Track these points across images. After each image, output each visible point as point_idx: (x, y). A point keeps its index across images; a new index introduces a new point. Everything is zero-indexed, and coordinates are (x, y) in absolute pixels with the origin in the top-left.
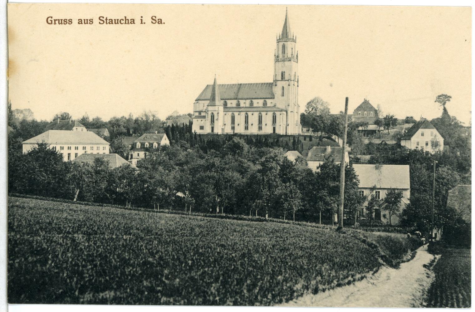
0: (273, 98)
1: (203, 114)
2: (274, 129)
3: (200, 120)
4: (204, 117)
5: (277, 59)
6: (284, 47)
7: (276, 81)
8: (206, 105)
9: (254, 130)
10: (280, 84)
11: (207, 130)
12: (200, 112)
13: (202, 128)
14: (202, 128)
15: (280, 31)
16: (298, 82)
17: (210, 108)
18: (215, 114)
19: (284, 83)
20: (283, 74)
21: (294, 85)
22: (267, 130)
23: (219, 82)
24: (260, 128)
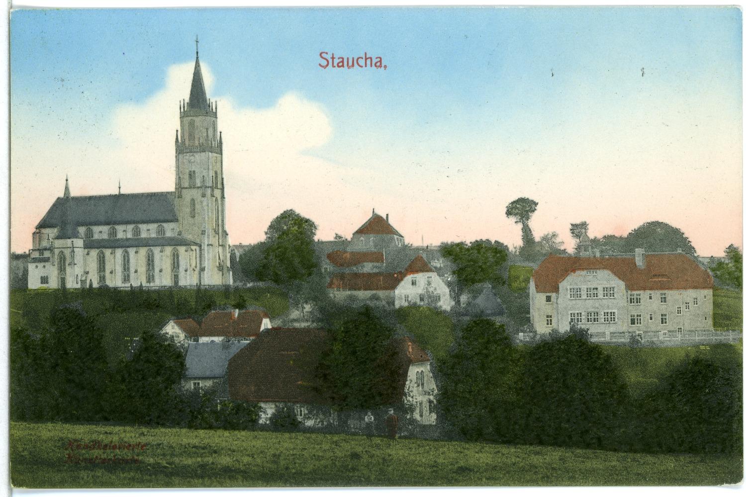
0: (175, 220)
1: (47, 254)
2: (176, 277)
3: (40, 265)
4: (46, 260)
5: (182, 149)
6: (192, 124)
7: (179, 187)
8: (52, 236)
9: (138, 280)
10: (188, 195)
11: (53, 284)
12: (41, 251)
13: (44, 280)
14: (44, 280)
15: (186, 95)
16: (223, 189)
17: (58, 243)
18: (67, 252)
19: (196, 194)
20: (192, 175)
21: (213, 196)
22: (163, 280)
23: (74, 193)
24: (150, 278)
